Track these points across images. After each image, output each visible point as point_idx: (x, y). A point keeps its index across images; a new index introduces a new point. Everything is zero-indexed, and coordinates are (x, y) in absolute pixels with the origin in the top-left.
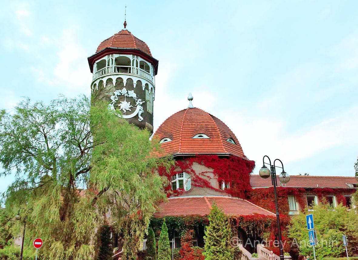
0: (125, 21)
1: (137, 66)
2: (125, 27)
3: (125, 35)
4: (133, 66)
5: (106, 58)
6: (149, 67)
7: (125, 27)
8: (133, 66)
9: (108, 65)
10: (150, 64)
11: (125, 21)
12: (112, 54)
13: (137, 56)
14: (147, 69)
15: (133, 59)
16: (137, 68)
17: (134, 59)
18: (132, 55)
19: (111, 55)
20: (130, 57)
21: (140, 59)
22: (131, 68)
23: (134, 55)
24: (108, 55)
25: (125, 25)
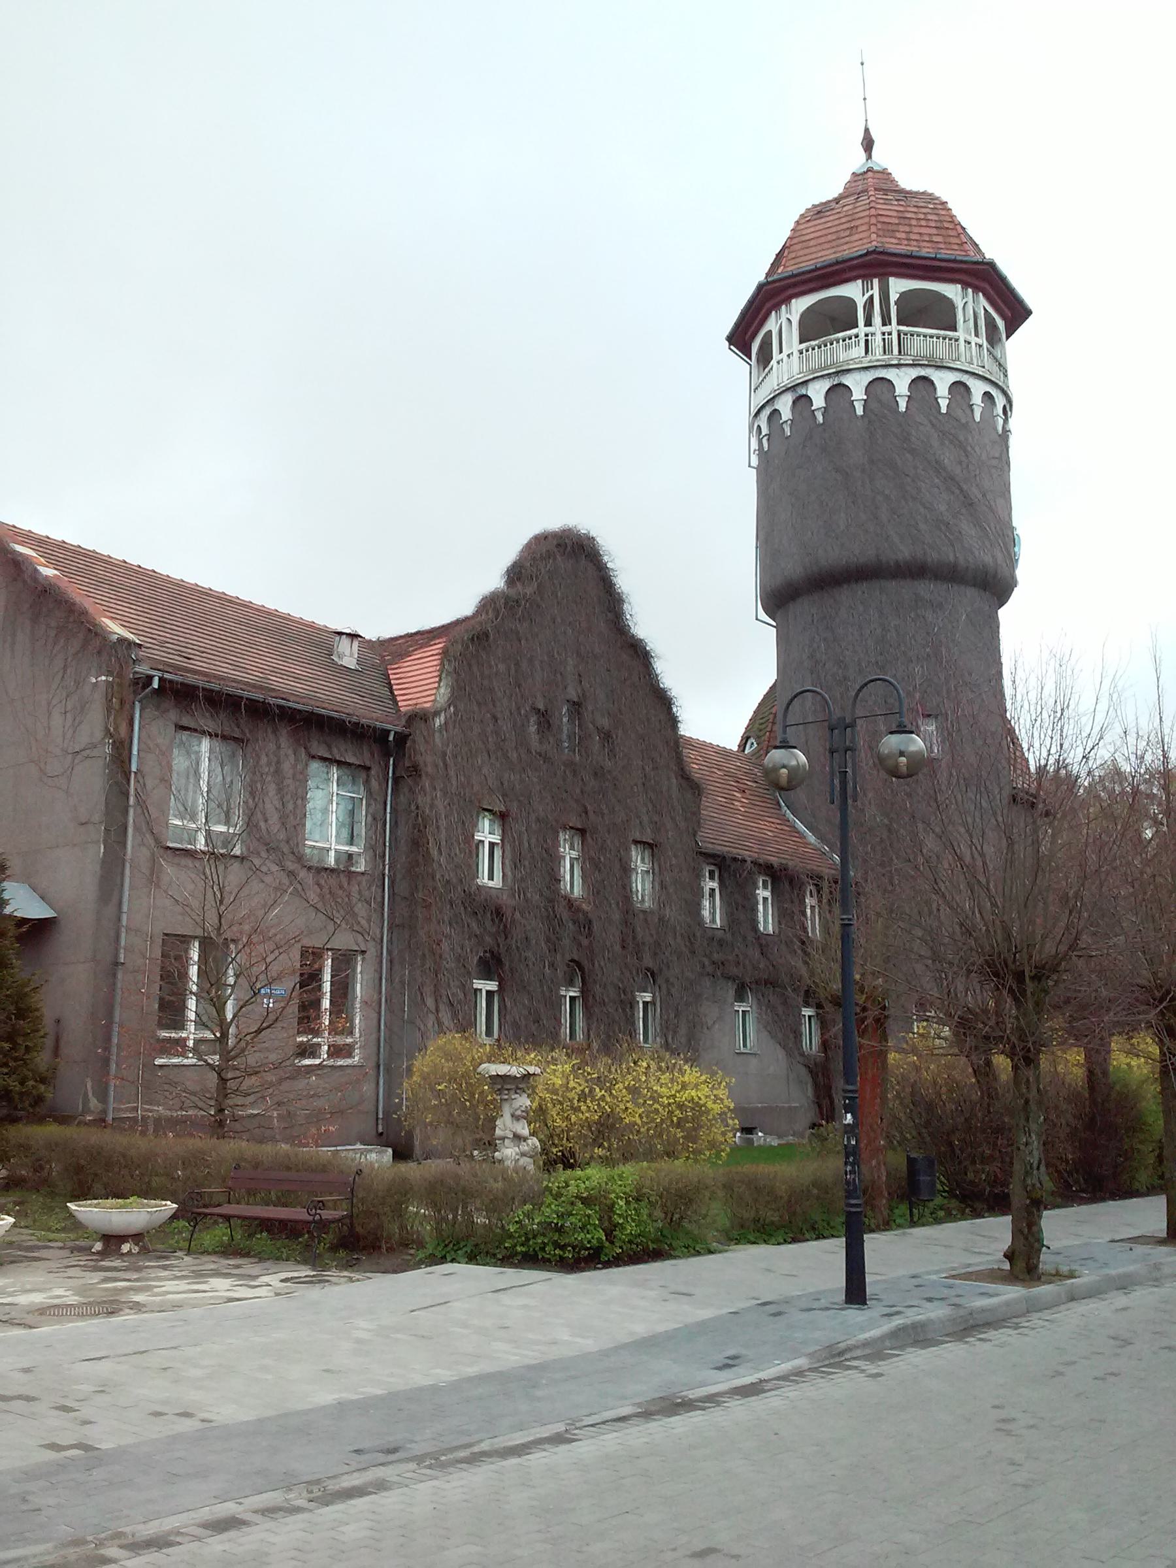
0: (867, 131)
1: (886, 321)
2: (869, 157)
3: (872, 185)
4: (868, 323)
5: (771, 325)
6: (949, 304)
7: (869, 157)
8: (868, 323)
9: (781, 352)
10: (951, 291)
11: (867, 131)
12: (787, 300)
13: (884, 278)
14: (939, 315)
15: (867, 296)
16: (887, 329)
17: (872, 296)
18: (859, 282)
19: (783, 307)
20: (853, 291)
21: (898, 286)
22: (862, 335)
23: (866, 277)
24: (777, 307)
25: (868, 144)
